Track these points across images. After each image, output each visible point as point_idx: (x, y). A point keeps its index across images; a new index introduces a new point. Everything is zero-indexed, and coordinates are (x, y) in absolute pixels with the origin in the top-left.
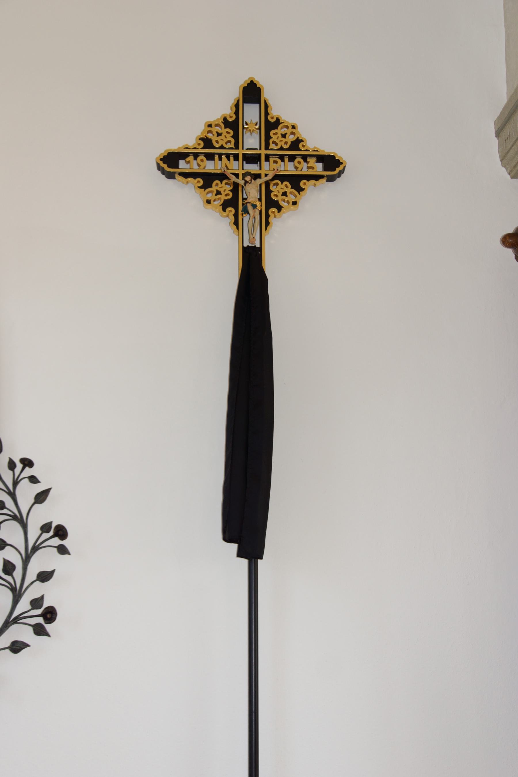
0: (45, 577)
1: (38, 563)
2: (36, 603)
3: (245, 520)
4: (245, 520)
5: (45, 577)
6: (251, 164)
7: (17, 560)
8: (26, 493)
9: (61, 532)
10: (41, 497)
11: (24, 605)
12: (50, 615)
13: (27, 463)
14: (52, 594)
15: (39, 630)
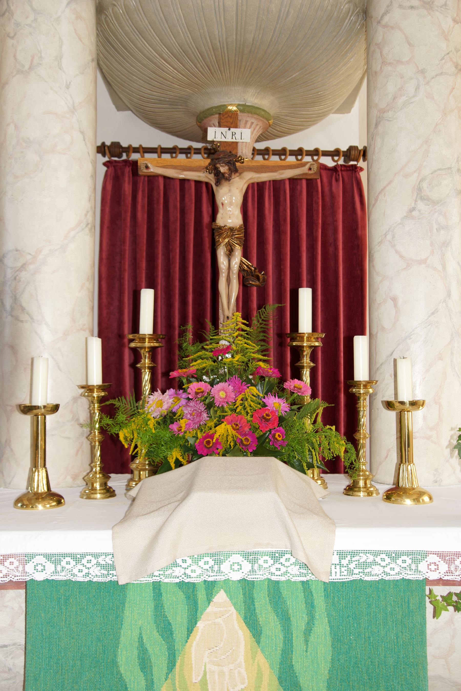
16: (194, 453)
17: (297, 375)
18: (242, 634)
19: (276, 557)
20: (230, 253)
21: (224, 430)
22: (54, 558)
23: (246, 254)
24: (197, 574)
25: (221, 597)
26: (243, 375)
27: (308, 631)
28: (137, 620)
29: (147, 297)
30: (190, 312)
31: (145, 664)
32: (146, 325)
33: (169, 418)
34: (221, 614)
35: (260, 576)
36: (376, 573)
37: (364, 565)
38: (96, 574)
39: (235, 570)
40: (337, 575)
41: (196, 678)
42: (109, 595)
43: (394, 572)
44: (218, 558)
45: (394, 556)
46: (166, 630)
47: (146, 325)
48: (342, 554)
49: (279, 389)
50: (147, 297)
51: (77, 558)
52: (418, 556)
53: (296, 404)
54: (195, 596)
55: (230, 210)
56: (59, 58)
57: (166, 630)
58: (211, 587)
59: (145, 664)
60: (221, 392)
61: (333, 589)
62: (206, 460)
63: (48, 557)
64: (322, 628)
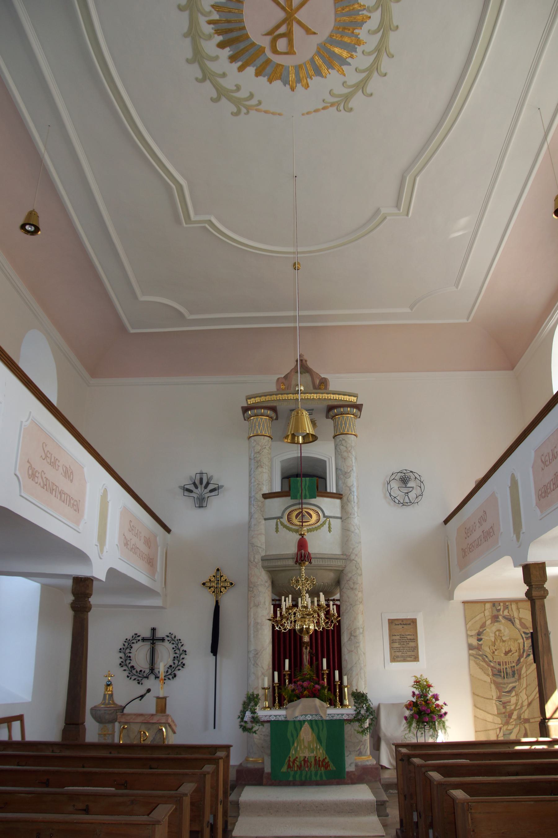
0: (183, 658)
1: (182, 657)
2: (182, 663)
3: (214, 650)
4: (214, 650)
5: (183, 658)
6: (218, 584)
7: (178, 656)
8: (180, 645)
9: (185, 651)
10: (182, 645)
11: (180, 663)
12: (184, 665)
13: (180, 640)
14: (184, 661)
15: (182, 667)
16: (299, 698)
17: (323, 680)
18: (310, 730)
19: (316, 715)
20: (306, 648)
21: (306, 692)
22: (276, 716)
23: (311, 648)
24: (302, 718)
25: (306, 723)
26: (310, 680)
27: (322, 729)
28: (291, 727)
29: (287, 661)
30: (297, 665)
31: (292, 736)
32: (287, 668)
33: (293, 690)
34: (306, 726)
35: (313, 719)
36: (335, 718)
37: (332, 716)
38: (283, 719)
39: (309, 718)
40: (327, 718)
41: (302, 738)
42: (285, 723)
43: (338, 717)
44: (306, 715)
45: (338, 715)
46: (296, 730)
47: (287, 668)
48: (328, 714)
49: (318, 684)
50: (287, 661)
51: (280, 716)
52: (342, 715)
53: (323, 688)
54: (302, 723)
55: (306, 639)
56: (265, 602)
57: (296, 730)
58: (304, 721)
59: (292, 736)
60: (305, 684)
61: (326, 721)
62: (302, 699)
63: (274, 716)
64: (325, 729)
